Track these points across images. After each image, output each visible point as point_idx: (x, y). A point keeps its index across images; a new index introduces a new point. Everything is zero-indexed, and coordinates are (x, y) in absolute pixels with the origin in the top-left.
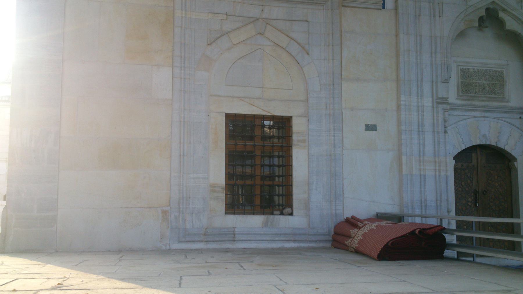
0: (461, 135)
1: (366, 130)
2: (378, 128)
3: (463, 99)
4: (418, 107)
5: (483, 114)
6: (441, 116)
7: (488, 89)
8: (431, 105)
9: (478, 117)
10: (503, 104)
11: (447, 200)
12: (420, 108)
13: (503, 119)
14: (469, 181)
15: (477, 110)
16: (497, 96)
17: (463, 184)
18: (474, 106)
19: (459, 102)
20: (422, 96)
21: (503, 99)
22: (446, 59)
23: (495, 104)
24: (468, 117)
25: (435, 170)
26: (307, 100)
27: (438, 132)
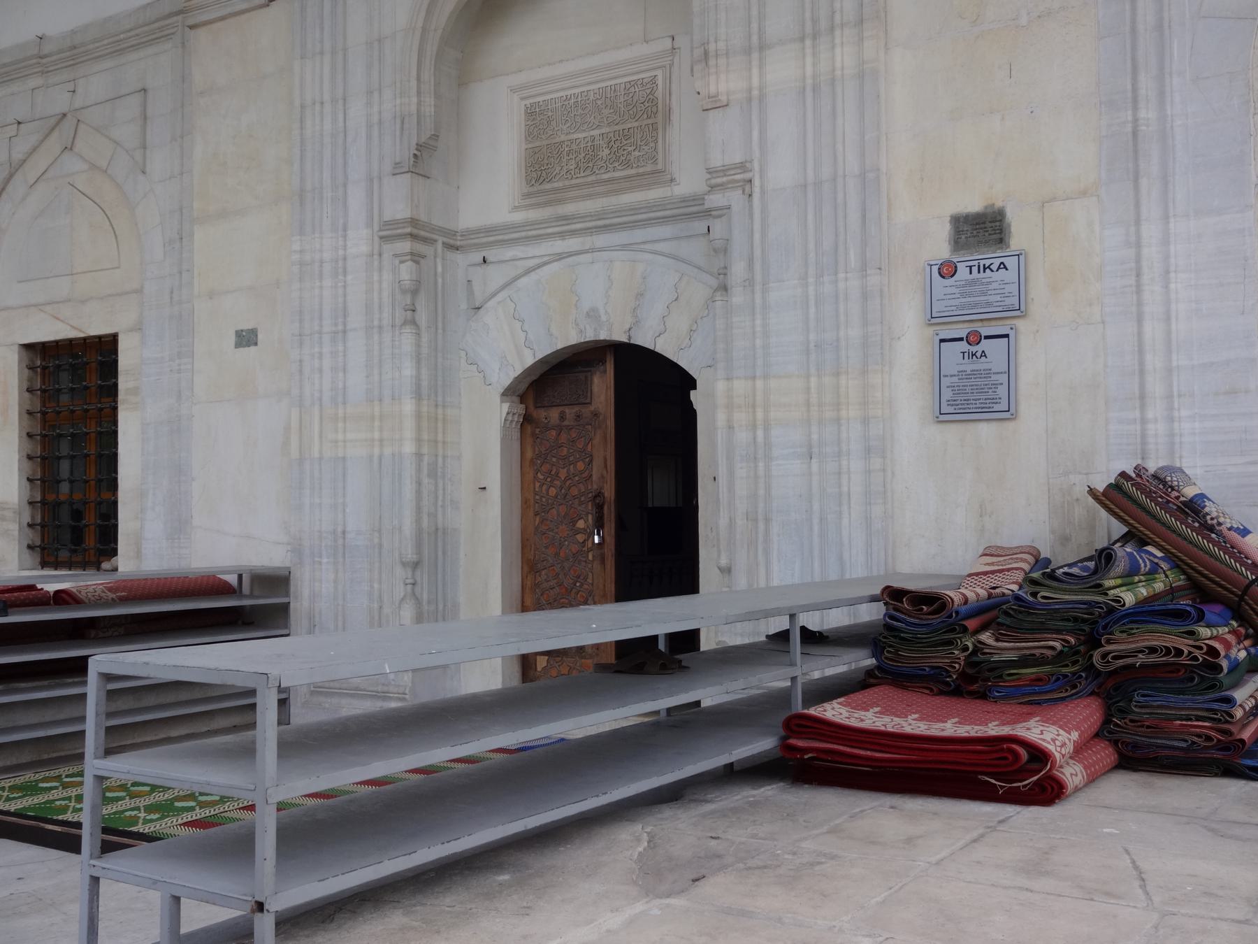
0: (523, 321)
1: (238, 345)
2: (260, 336)
6: (387, 276)
7: (607, 151)
8: (364, 249)
9: (570, 254)
10: (654, 194)
14: (581, 466)
15: (573, 233)
16: (633, 172)
18: (566, 219)
19: (519, 217)
20: (345, 230)
21: (659, 176)
22: (398, 101)
23: (628, 199)
24: (537, 261)
25: (373, 440)
26: (139, 291)
27: (380, 327)
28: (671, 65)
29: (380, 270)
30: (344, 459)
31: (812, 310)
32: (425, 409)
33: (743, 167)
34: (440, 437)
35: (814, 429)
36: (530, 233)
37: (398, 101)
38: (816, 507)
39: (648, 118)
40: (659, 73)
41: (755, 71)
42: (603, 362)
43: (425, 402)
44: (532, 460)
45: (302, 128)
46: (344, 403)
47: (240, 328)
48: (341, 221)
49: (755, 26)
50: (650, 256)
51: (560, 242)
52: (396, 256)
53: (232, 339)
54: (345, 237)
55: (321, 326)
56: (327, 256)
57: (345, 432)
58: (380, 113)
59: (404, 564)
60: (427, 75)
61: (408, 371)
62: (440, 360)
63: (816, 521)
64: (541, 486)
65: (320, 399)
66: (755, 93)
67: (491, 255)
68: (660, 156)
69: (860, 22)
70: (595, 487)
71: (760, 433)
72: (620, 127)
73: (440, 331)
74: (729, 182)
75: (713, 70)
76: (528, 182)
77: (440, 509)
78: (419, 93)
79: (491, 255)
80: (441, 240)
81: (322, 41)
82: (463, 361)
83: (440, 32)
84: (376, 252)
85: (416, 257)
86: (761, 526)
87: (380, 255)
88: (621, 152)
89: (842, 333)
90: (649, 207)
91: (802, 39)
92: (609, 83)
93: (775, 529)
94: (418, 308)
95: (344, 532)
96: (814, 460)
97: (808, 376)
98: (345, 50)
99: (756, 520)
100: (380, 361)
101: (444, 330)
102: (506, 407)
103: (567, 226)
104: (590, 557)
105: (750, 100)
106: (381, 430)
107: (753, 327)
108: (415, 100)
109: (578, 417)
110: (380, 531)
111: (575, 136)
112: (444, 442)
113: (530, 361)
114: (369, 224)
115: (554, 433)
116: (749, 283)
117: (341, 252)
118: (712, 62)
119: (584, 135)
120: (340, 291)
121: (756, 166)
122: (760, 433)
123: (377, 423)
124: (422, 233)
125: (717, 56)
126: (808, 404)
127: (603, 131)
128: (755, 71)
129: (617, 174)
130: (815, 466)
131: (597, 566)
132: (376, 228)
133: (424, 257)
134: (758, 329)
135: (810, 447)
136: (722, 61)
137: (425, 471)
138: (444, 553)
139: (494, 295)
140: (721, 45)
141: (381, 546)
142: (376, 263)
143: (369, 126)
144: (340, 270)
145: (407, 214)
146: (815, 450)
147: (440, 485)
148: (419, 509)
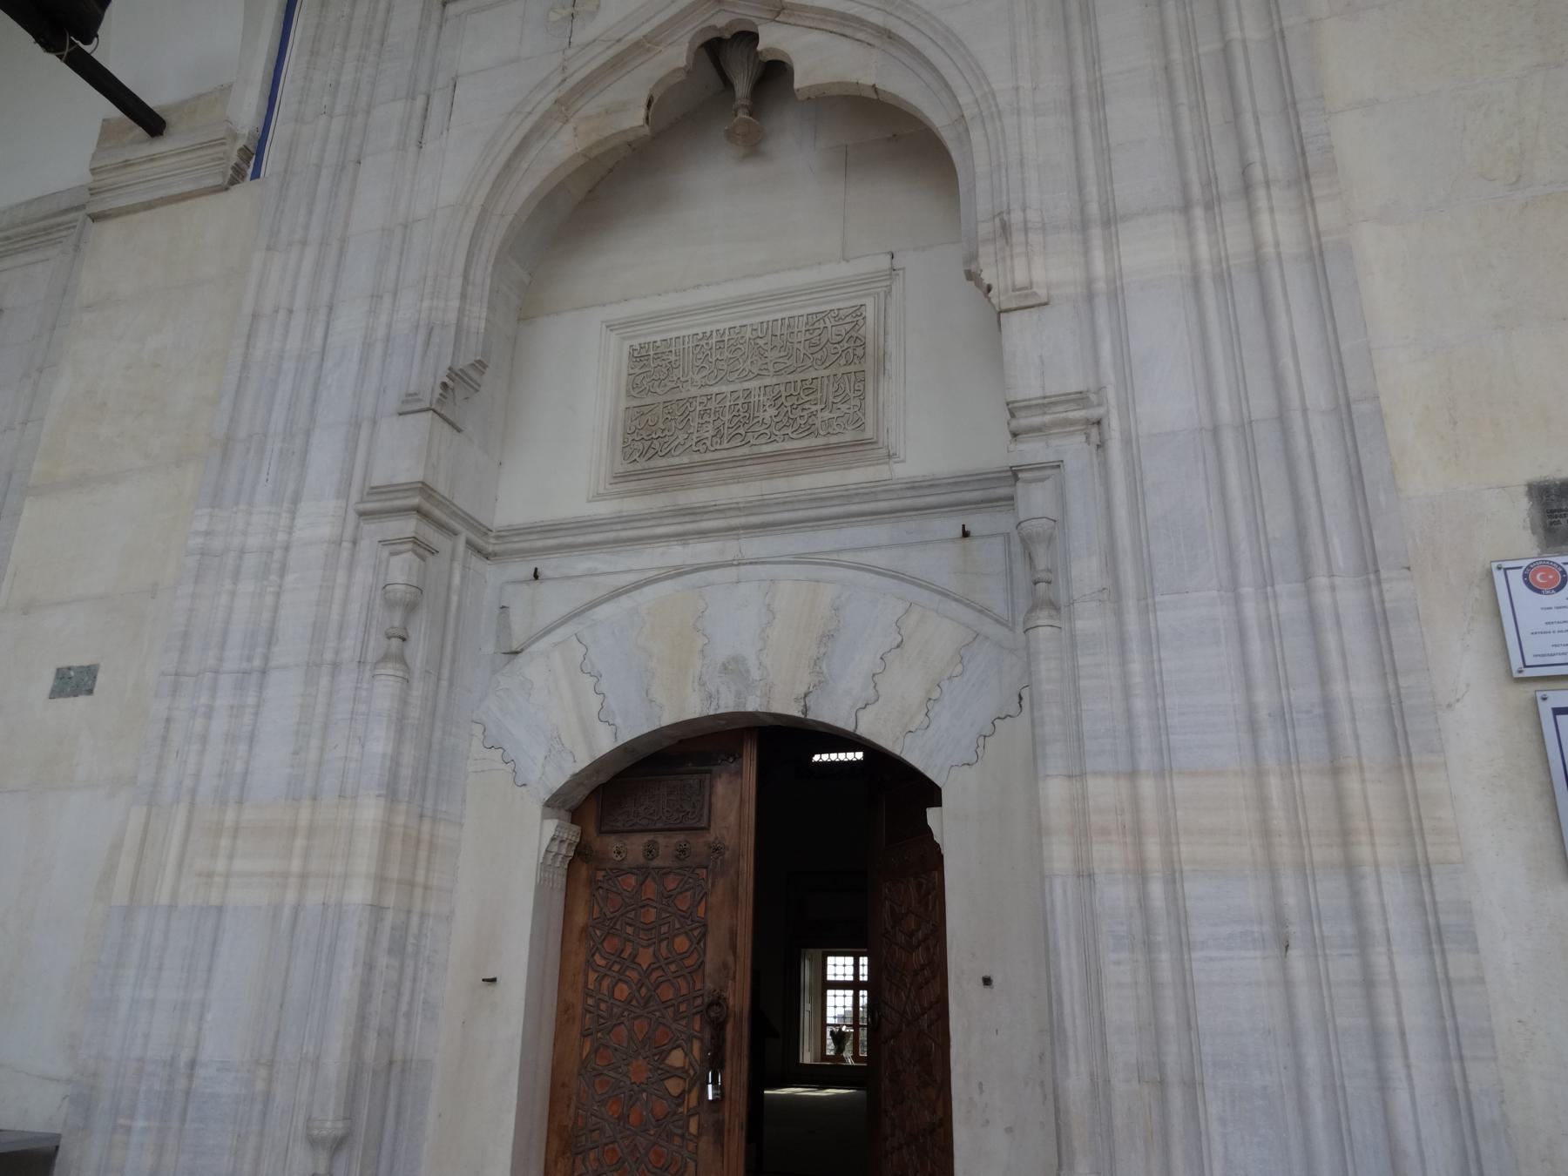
0: (598, 677)
1: (56, 693)
2: (101, 678)
3: (630, 494)
4: (271, 553)
5: (730, 548)
6: (362, 576)
7: (772, 412)
8: (326, 531)
9: (697, 570)
10: (858, 475)
11: (317, 1064)
12: (278, 555)
13: (846, 557)
14: (681, 943)
15: (702, 534)
16: (820, 441)
17: (646, 957)
19: (604, 509)
20: (296, 500)
21: (863, 447)
22: (426, 304)
28: (888, 293)
29: (351, 566)
30: (220, 909)
31: (1256, 647)
32: (400, 820)
33: (1081, 399)
34: (420, 877)
35: (1288, 883)
36: (624, 534)
37: (426, 304)
38: (1312, 1059)
39: (847, 363)
40: (869, 302)
41: (1098, 255)
42: (737, 756)
43: (402, 807)
44: (584, 929)
45: (248, 345)
46: (240, 802)
47: (64, 664)
48: (291, 487)
49: (1092, 190)
50: (851, 574)
51: (680, 548)
52: (385, 543)
53: (48, 680)
54: (293, 513)
55: (220, 659)
56: (253, 542)
57: (231, 857)
58: (389, 326)
59: (313, 1142)
60: (490, 268)
61: (379, 743)
62: (438, 734)
63: (1315, 1092)
64: (599, 981)
65: (193, 792)
66: (1100, 285)
67: (548, 566)
68: (870, 420)
69: (1302, 178)
70: (709, 985)
71: (1157, 890)
72: (798, 377)
73: (444, 683)
74: (1056, 424)
75: (1018, 250)
76: (628, 453)
77: (402, 1021)
78: (463, 296)
79: (548, 566)
80: (465, 534)
81: (307, 227)
82: (477, 743)
83: (510, 218)
84: (348, 534)
85: (422, 548)
86: (1176, 1097)
87: (355, 542)
88: (798, 412)
89: (1338, 689)
90: (847, 495)
91: (1186, 208)
92: (779, 316)
93: (1214, 1108)
94: (413, 636)
95: (192, 1064)
96: (1294, 953)
97: (1259, 774)
98: (343, 241)
99: (1162, 1083)
100: (325, 727)
101: (451, 684)
102: (551, 827)
103: (691, 524)
104: (693, 1128)
105: (1090, 297)
106: (307, 854)
107: (1125, 675)
108: (455, 304)
109: (682, 852)
110: (271, 1065)
111: (715, 390)
112: (426, 887)
113: (606, 743)
114: (343, 492)
115: (632, 880)
116: (1114, 593)
117: (281, 537)
118: (1017, 238)
119: (732, 387)
120: (269, 600)
121: (1111, 394)
122: (1157, 890)
123: (300, 842)
124: (437, 513)
125: (1026, 230)
126: (1266, 832)
127: (767, 381)
128: (1098, 255)
129: (788, 445)
130: (1298, 962)
131: (705, 1143)
132: (354, 497)
133: (434, 552)
134: (1137, 679)
135: (1280, 920)
136: (1035, 238)
137: (385, 942)
138: (398, 1114)
139: (548, 631)
140: (1032, 215)
141: (268, 1097)
142: (345, 555)
143: (367, 345)
144: (275, 566)
145: (418, 475)
146: (1296, 930)
147: (409, 971)
148: (362, 1018)
